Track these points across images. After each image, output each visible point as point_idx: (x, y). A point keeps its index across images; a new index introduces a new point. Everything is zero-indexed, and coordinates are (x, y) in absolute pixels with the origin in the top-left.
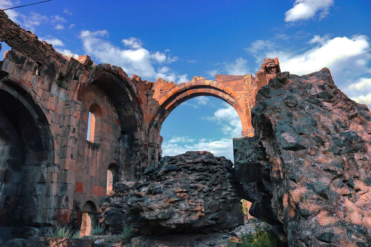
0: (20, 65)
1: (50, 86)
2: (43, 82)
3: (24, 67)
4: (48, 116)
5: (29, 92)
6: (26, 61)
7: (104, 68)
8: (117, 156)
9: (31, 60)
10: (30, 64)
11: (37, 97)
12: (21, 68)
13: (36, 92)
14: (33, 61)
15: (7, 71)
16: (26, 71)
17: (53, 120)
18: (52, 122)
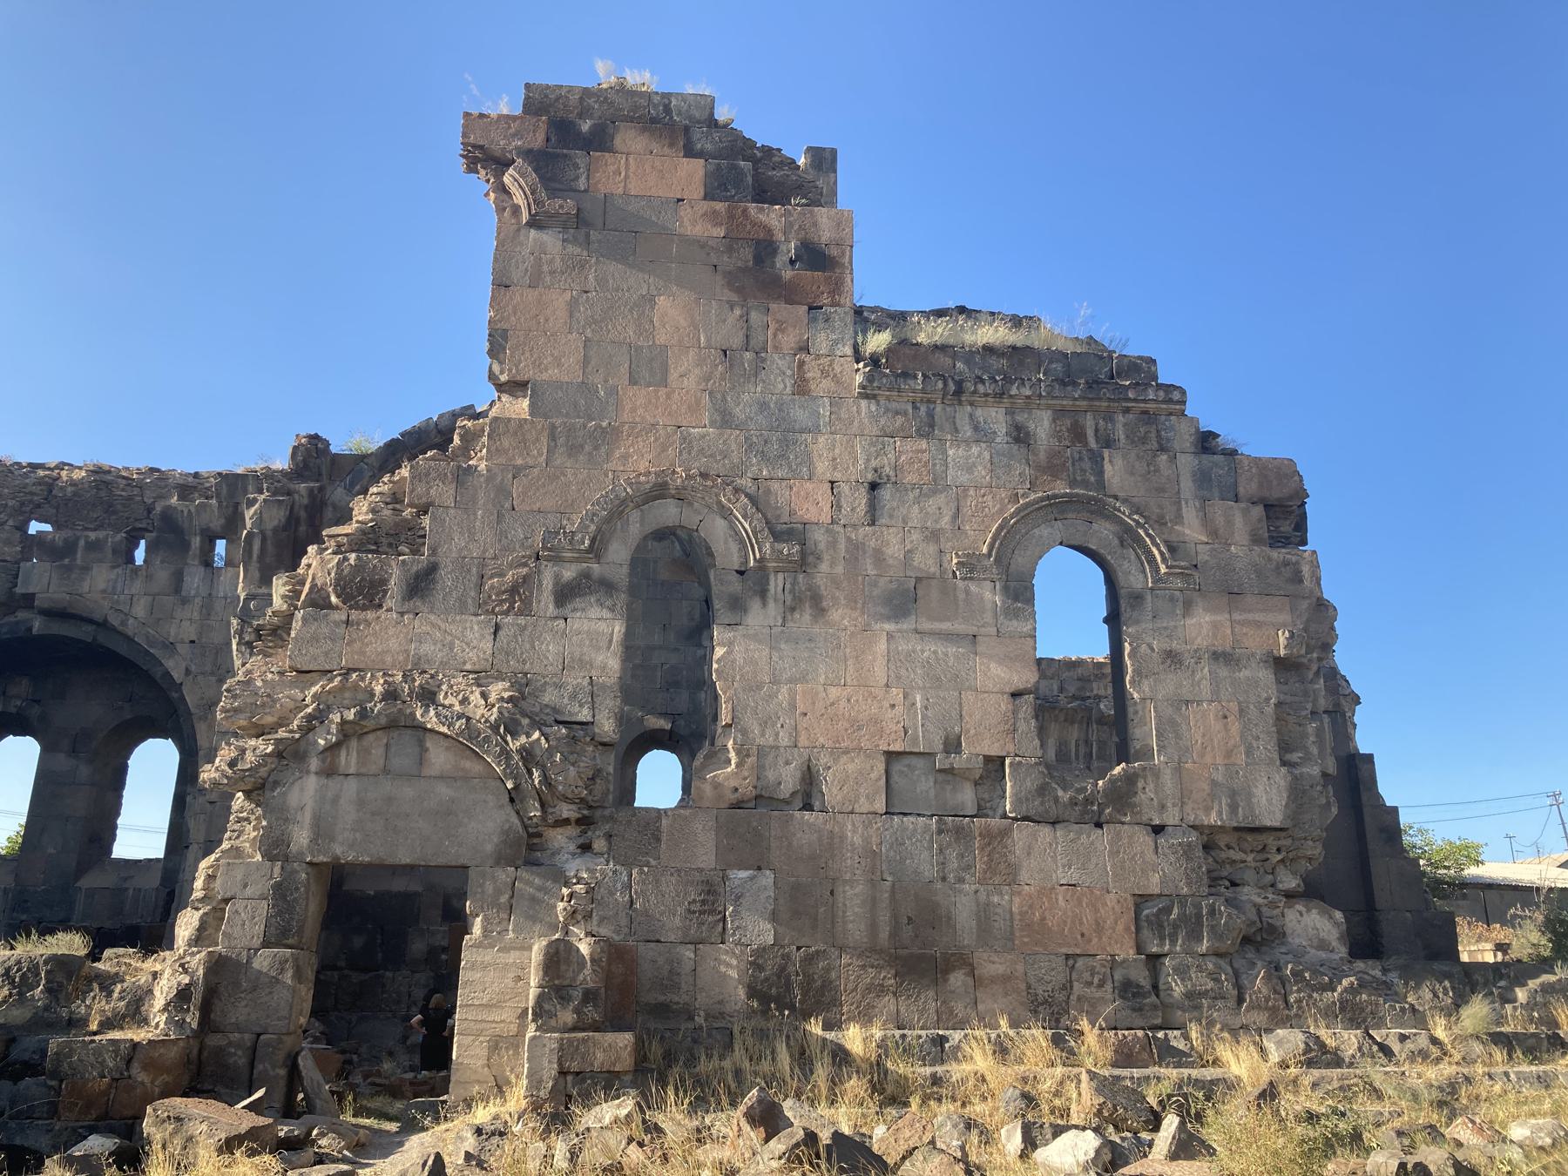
0: (66, 561)
1: (178, 578)
2: (149, 577)
3: (79, 562)
4: (169, 664)
5: (97, 617)
6: (82, 543)
7: (439, 432)
8: (685, 695)
9: (92, 535)
10: (93, 546)
11: (131, 621)
12: (69, 569)
13: (126, 609)
14: (101, 534)
15: (31, 590)
16: (86, 569)
17: (193, 668)
18: (188, 672)
